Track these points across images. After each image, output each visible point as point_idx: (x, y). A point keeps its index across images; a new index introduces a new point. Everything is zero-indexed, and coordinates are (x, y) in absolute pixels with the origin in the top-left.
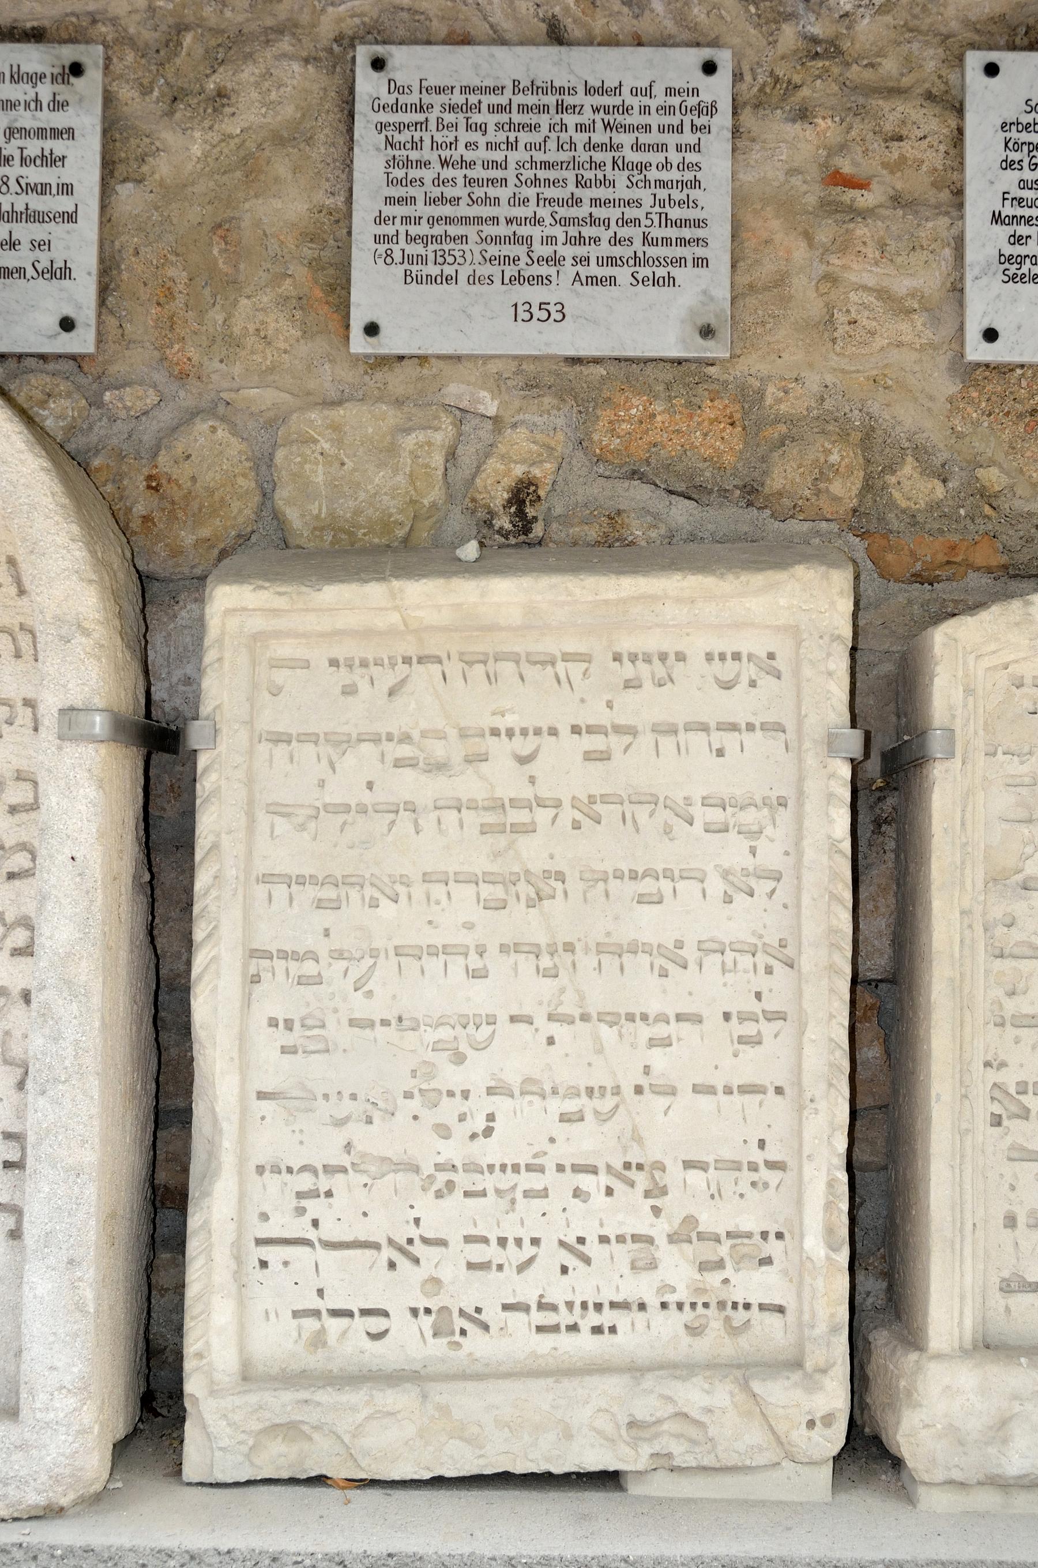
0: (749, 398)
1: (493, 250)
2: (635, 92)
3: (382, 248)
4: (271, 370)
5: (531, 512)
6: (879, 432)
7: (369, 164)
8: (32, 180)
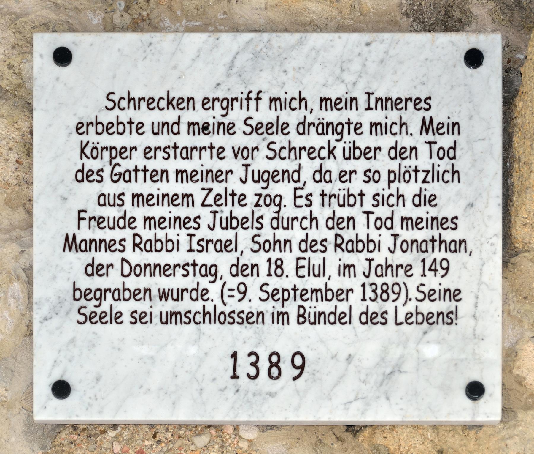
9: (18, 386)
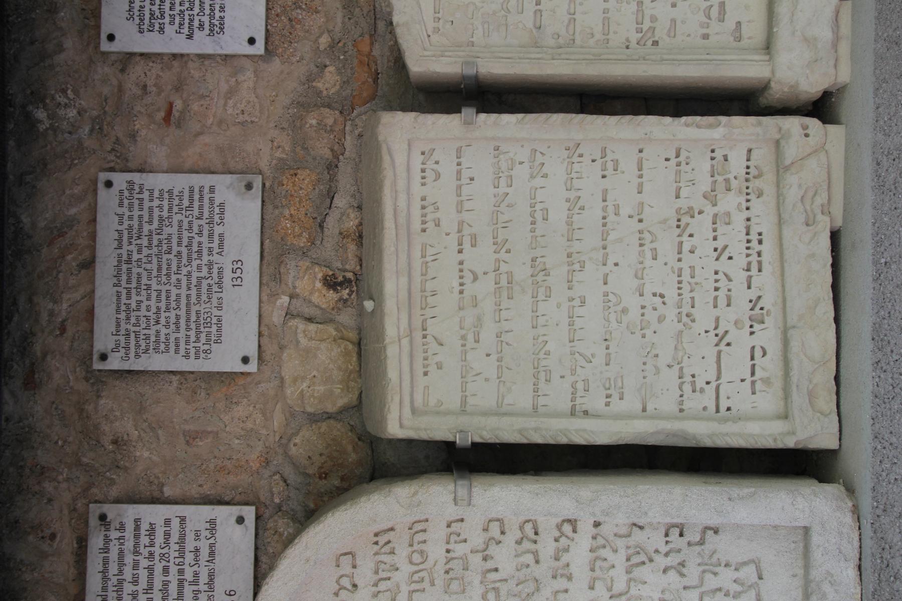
0: (282, 167)
1: (204, 297)
2: (121, 223)
3: (202, 355)
4: (264, 414)
5: (340, 279)
6: (300, 99)
7: (157, 362)
8: (163, 541)
9: (248, 64)
